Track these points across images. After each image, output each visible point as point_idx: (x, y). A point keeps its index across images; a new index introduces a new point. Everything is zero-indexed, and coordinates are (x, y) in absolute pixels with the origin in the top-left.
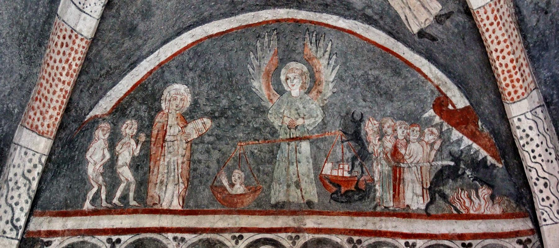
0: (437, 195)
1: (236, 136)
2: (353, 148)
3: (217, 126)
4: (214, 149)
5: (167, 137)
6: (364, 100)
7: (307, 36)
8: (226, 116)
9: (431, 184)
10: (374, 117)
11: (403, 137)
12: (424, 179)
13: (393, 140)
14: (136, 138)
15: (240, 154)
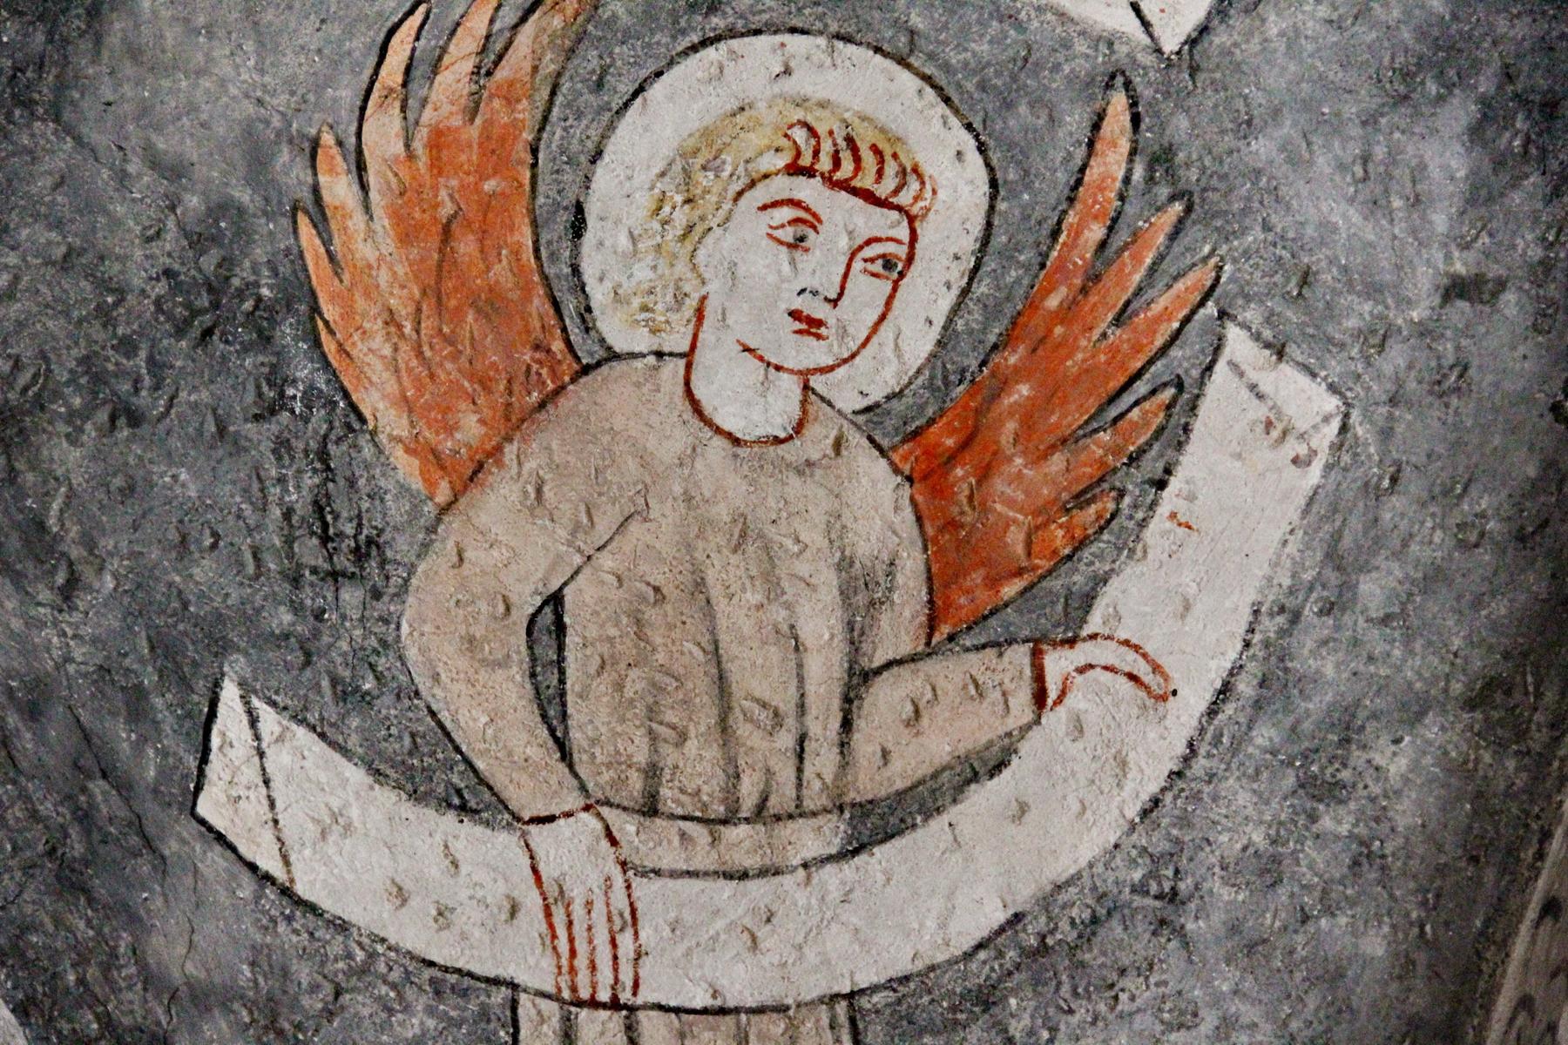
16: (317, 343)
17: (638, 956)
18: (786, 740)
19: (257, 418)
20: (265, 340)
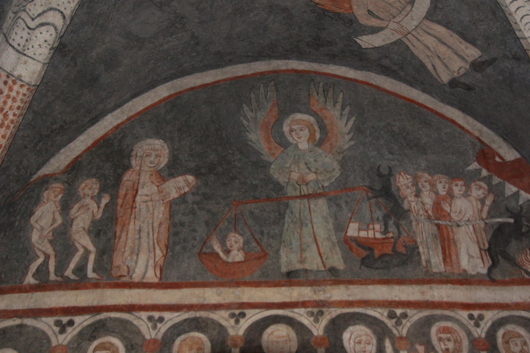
0: (500, 257)
1: (229, 194)
2: (382, 205)
3: (204, 184)
4: (200, 209)
5: (138, 198)
6: (391, 153)
7: (312, 86)
8: (215, 172)
9: (490, 244)
10: (406, 172)
11: (444, 193)
12: (480, 239)
13: (434, 196)
14: (98, 199)
15: (235, 215)
16: (329, 12)
17: (406, 28)
18: (398, 3)
19: (332, 20)
20: (326, 15)
